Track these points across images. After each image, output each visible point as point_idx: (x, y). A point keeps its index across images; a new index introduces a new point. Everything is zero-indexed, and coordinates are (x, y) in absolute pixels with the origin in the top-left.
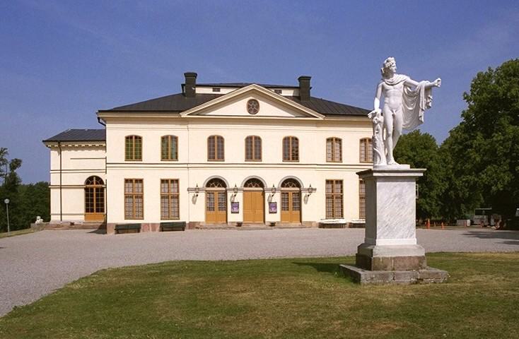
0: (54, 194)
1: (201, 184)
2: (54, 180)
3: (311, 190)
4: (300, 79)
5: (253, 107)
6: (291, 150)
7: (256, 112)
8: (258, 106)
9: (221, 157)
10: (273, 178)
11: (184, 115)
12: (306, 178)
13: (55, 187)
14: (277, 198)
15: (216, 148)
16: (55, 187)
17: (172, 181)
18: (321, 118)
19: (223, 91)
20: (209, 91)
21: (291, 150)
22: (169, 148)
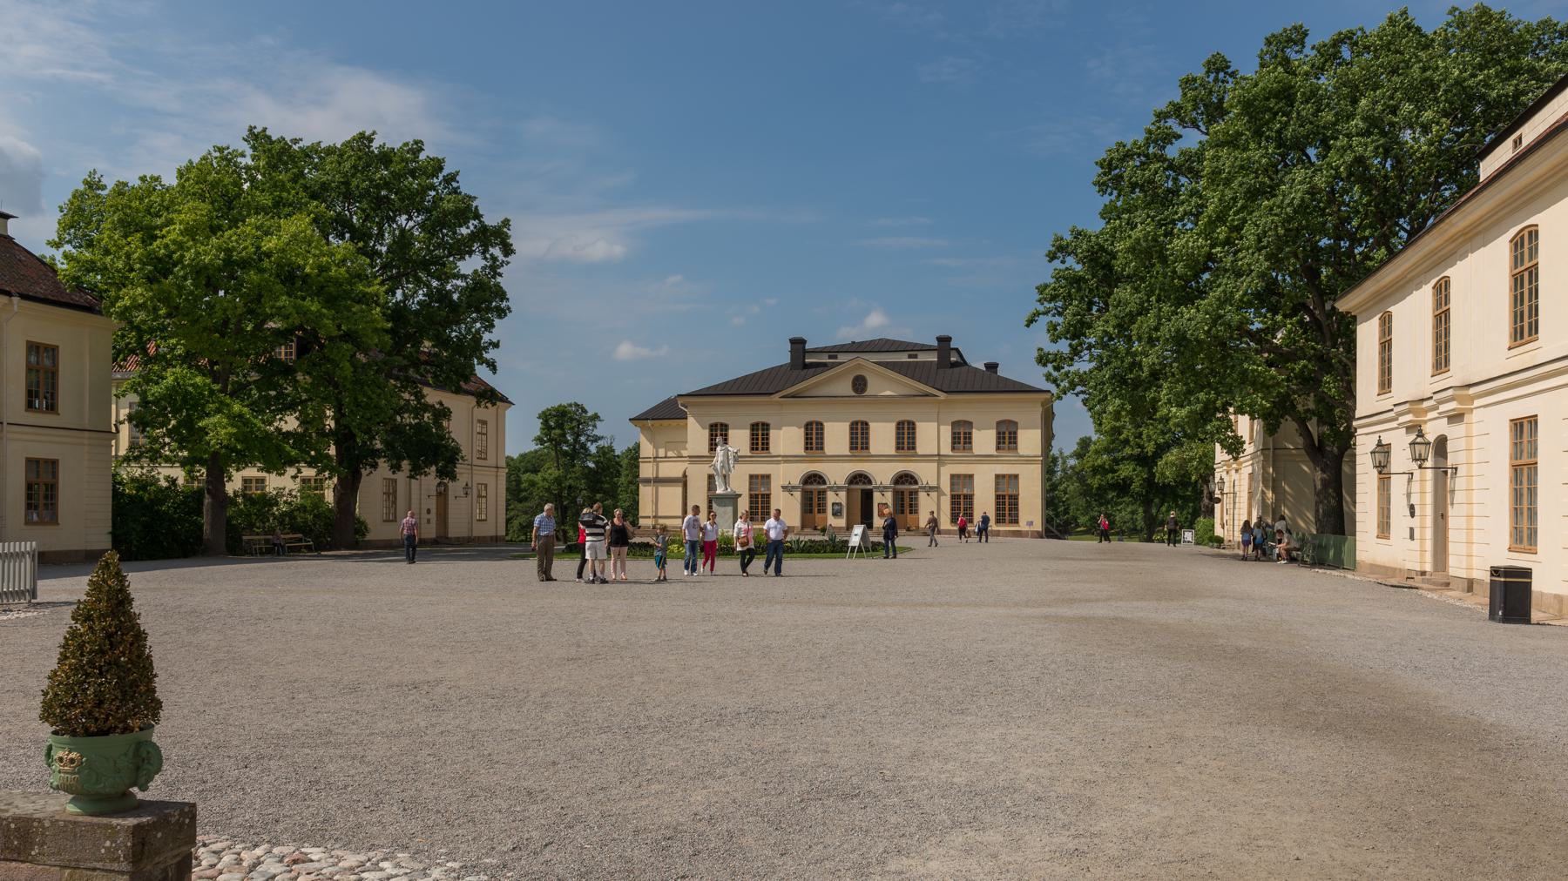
0: (645, 492)
1: (796, 482)
2: (646, 471)
3: (929, 489)
4: (940, 339)
5: (860, 384)
6: (906, 437)
7: (863, 390)
8: (865, 385)
9: (821, 447)
10: (883, 474)
11: (776, 398)
12: (925, 472)
13: (647, 481)
14: (888, 498)
15: (814, 438)
16: (647, 481)
17: (763, 476)
18: (943, 396)
19: (842, 358)
20: (825, 359)
21: (906, 437)
22: (760, 438)
